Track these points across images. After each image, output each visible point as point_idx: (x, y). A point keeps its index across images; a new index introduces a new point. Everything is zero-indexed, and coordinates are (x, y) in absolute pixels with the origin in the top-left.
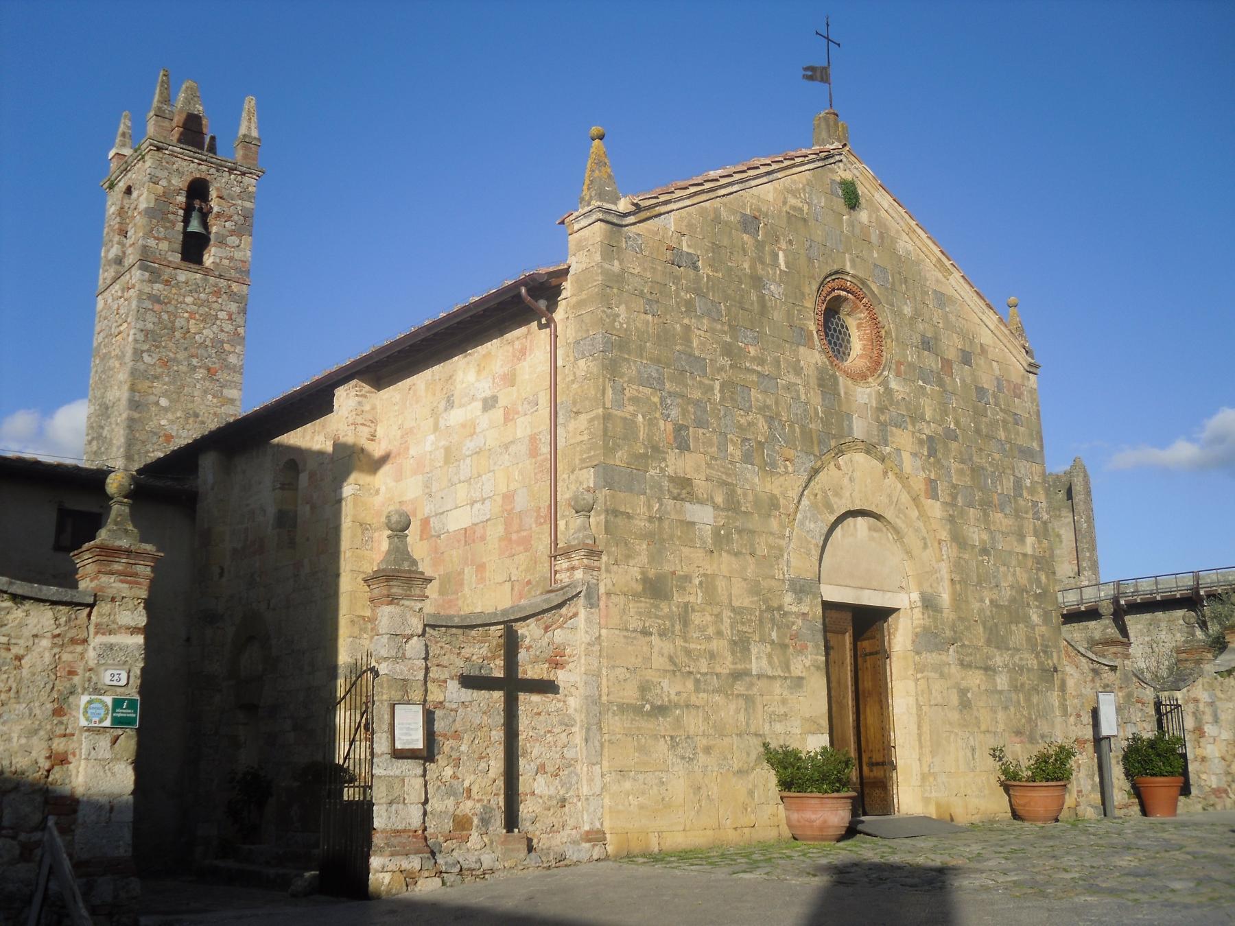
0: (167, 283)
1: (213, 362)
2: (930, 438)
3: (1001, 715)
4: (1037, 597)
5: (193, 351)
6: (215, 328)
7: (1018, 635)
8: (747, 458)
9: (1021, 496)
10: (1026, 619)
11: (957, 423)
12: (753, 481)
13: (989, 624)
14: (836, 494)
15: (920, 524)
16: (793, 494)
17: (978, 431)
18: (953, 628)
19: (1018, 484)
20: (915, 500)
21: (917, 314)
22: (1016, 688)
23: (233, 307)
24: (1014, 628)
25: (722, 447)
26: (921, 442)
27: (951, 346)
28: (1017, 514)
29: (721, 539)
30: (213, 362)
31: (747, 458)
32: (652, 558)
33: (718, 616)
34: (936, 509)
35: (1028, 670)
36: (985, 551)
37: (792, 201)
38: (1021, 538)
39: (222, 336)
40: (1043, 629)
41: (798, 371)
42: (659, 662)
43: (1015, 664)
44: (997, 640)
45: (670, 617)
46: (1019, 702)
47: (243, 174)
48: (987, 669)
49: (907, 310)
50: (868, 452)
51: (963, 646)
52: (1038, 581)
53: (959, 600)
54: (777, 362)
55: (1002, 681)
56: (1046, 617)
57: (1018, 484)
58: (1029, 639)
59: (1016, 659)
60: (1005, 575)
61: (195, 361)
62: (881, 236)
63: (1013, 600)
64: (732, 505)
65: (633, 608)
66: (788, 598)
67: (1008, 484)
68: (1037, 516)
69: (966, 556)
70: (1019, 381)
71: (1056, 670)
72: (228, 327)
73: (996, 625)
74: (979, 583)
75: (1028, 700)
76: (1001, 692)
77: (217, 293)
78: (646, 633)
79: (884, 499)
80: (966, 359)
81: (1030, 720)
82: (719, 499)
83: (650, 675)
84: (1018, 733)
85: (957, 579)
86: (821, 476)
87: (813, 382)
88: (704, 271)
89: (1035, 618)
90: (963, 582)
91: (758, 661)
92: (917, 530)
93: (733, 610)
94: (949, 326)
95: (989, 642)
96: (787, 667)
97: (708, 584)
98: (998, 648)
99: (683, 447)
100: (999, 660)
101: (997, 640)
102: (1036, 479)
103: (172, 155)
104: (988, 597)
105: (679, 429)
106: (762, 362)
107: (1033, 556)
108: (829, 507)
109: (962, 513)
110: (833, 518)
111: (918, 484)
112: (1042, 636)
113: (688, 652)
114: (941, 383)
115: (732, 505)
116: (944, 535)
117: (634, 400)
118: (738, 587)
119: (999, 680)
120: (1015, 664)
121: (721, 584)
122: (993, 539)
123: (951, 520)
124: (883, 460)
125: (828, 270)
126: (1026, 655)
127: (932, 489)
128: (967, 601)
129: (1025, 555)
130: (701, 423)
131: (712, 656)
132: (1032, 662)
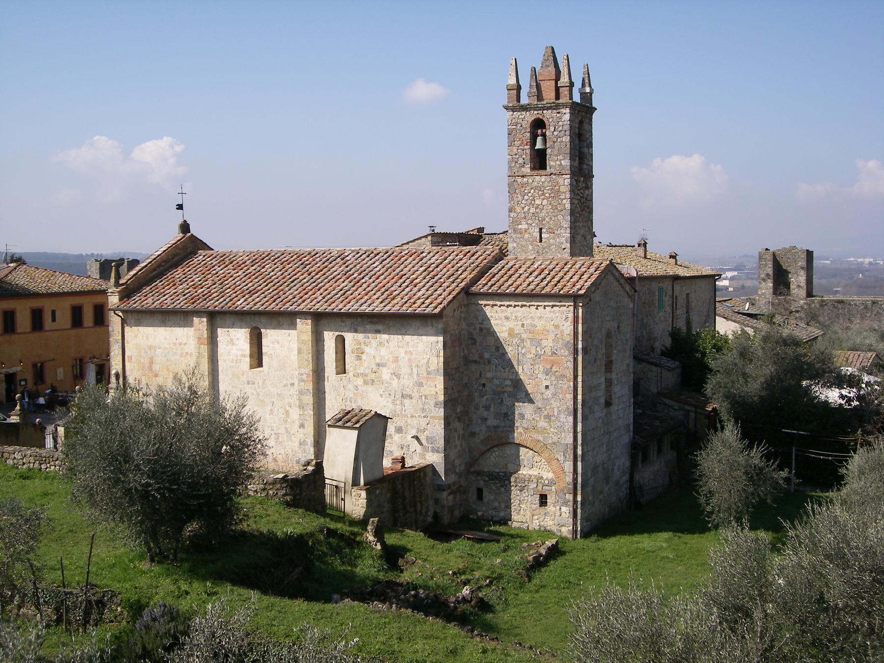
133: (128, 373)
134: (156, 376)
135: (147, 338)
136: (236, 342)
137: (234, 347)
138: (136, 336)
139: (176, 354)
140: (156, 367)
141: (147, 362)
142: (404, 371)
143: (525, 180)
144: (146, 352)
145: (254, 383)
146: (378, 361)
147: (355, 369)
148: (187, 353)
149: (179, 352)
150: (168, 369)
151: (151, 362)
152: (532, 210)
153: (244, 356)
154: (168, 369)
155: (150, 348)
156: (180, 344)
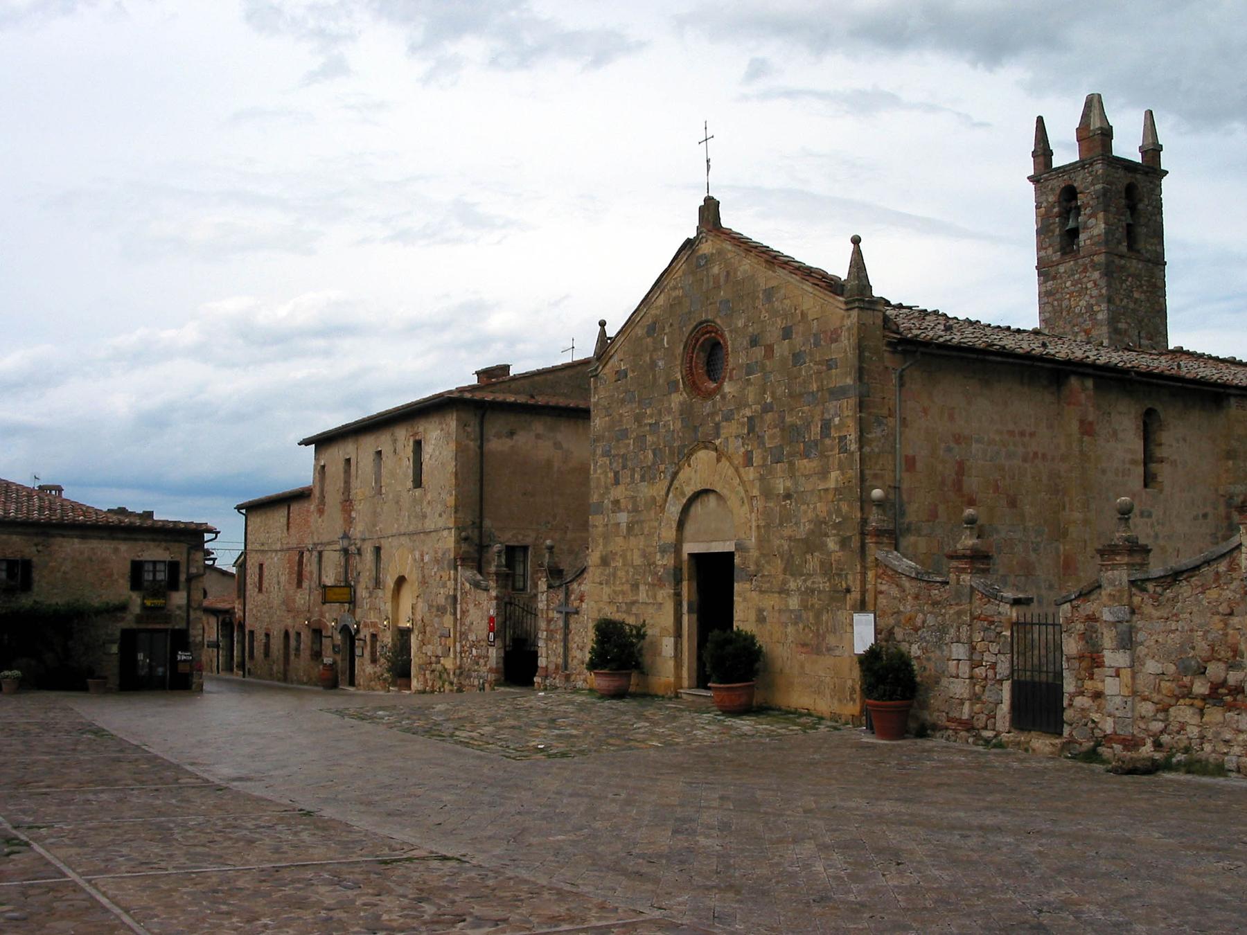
0: (1054, 278)
1: (1088, 325)
2: (750, 419)
3: (790, 629)
4: (836, 526)
5: (1075, 322)
6: (1087, 298)
7: (813, 562)
8: (643, 479)
9: (828, 436)
10: (822, 547)
11: (773, 394)
12: (647, 491)
13: (786, 557)
14: (688, 485)
15: (741, 489)
16: (663, 493)
17: (791, 395)
18: (757, 564)
19: (826, 426)
20: (737, 470)
24: (809, 557)
25: (632, 477)
26: (743, 424)
27: (773, 334)
28: (823, 456)
29: (630, 528)
30: (1088, 325)
31: (643, 479)
32: (605, 545)
33: (627, 572)
34: (750, 474)
35: (820, 592)
36: (788, 496)
37: (675, 294)
38: (824, 474)
39: (1093, 301)
40: (840, 554)
41: (669, 410)
42: (605, 598)
43: (807, 588)
44: (791, 569)
45: (609, 575)
46: (808, 619)
47: (1091, 164)
48: (779, 593)
49: (740, 324)
50: (706, 448)
51: (763, 576)
52: (838, 511)
53: (761, 541)
54: (660, 411)
55: (794, 603)
56: (844, 543)
57: (826, 426)
58: (822, 563)
59: (809, 583)
60: (805, 512)
61: (1076, 329)
62: (728, 273)
63: (812, 532)
64: (635, 510)
65: (599, 571)
66: (658, 556)
67: (816, 430)
68: (843, 449)
69: (771, 505)
70: (838, 324)
72: (1095, 292)
73: (793, 556)
74: (781, 524)
75: (818, 616)
76: (792, 611)
77: (1085, 270)
78: (601, 584)
79: (717, 478)
80: (787, 333)
81: (817, 634)
82: (630, 507)
83: (601, 605)
84: (804, 645)
85: (762, 523)
86: (681, 475)
87: (677, 414)
88: (630, 375)
89: (832, 544)
90: (767, 526)
91: (642, 596)
92: (737, 493)
93: (633, 567)
94: (774, 313)
95: (785, 571)
96: (655, 598)
97: (624, 557)
98: (792, 575)
99: (617, 482)
100: (792, 585)
101: (791, 569)
102: (846, 414)
103: (1046, 180)
105: (616, 473)
106: (651, 416)
107: (836, 489)
108: (683, 494)
109: (770, 472)
110: (684, 501)
112: (838, 562)
113: (615, 592)
114: (763, 368)
115: (635, 510)
116: (756, 492)
117: (601, 466)
118: (637, 553)
119: (791, 602)
120: (807, 588)
121: (629, 554)
122: (796, 484)
123: (762, 478)
124: (716, 450)
125: (691, 327)
127: (748, 461)
128: (769, 541)
129: (826, 490)
130: (624, 467)
131: (623, 593)
132: (822, 583)
135: (951, 418)
136: (1121, 435)
138: (925, 411)
140: (972, 483)
143: (1123, 262)
144: (949, 450)
145: (1150, 516)
148: (1036, 454)
151: (961, 469)
152: (1132, 306)
153: (1133, 462)
155: (958, 439)
156: (1022, 434)
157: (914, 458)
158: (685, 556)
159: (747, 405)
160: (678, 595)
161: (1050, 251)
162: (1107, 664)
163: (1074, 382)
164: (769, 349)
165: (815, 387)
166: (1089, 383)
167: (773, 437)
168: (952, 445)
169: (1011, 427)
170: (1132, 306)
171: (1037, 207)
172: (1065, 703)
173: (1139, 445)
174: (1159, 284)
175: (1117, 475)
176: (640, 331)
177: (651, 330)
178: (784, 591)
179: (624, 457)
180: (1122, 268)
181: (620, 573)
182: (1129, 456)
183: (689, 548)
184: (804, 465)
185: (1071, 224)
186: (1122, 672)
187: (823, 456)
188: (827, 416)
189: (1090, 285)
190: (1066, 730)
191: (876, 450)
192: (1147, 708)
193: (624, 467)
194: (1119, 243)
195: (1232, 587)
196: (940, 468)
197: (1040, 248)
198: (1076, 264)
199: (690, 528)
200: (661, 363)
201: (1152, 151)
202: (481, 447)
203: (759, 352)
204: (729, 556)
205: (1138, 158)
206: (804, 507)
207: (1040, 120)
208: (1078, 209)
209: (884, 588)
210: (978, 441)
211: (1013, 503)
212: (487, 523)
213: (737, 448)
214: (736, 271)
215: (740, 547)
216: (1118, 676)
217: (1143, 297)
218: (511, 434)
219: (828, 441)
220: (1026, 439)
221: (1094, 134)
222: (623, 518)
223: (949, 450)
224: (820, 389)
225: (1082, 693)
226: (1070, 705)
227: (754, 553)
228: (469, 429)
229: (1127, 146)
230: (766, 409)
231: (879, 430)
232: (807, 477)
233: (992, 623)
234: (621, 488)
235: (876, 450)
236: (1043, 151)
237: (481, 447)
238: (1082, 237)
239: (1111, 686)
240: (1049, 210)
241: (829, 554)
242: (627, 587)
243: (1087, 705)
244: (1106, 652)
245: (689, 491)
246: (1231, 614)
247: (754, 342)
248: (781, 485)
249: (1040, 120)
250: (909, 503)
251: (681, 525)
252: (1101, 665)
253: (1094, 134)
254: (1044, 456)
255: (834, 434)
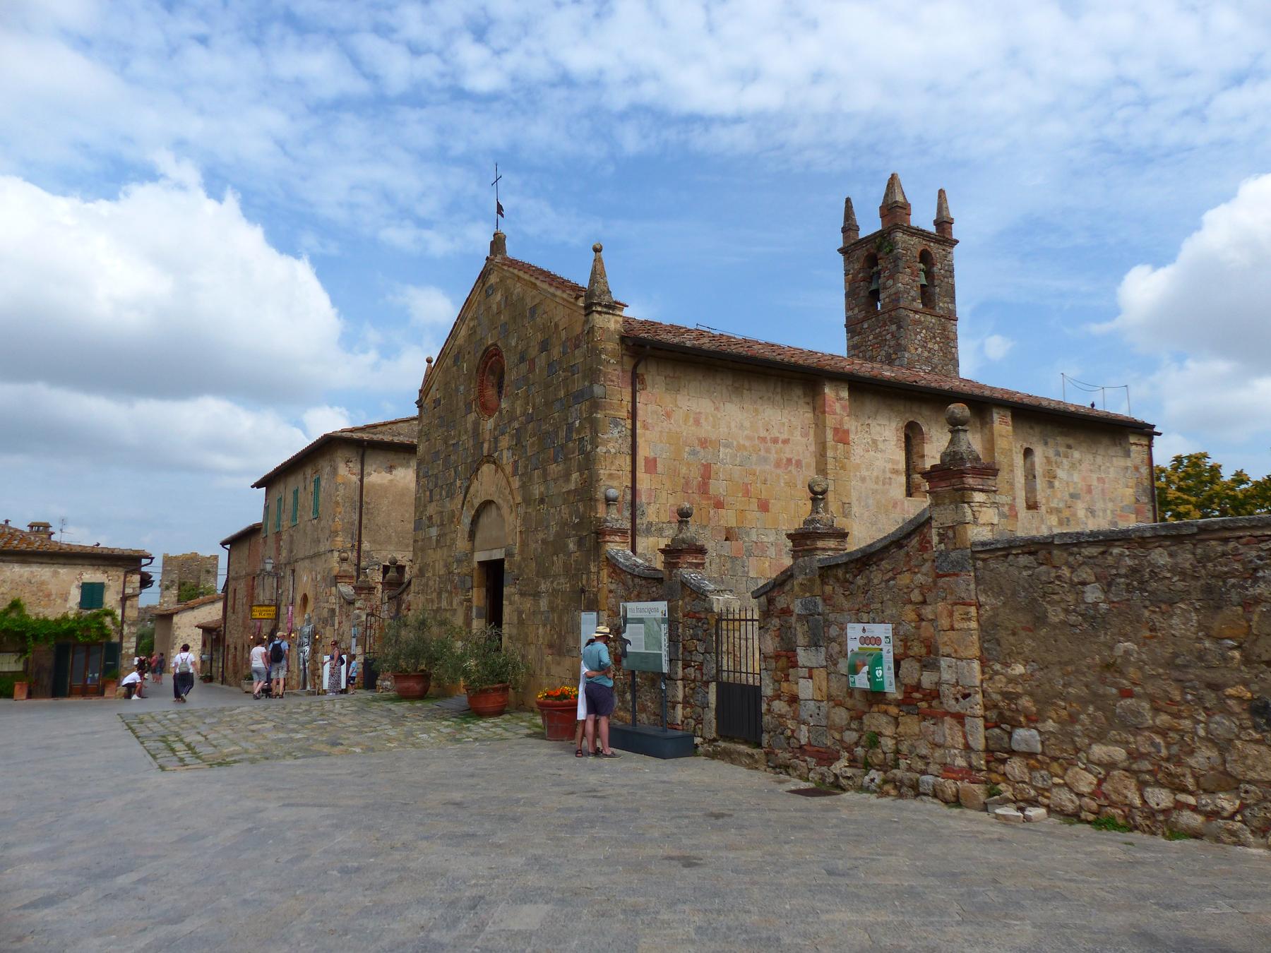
0: (859, 334)
7: (559, 561)
21: (519, 338)
22: (552, 609)
23: (894, 327)
28: (566, 459)
29: (438, 541)
34: (516, 483)
36: (542, 501)
38: (567, 476)
43: (554, 590)
55: (544, 604)
56: (580, 543)
63: (557, 534)
67: (562, 434)
68: (582, 451)
71: (583, 591)
75: (560, 618)
80: (545, 346)
81: (560, 636)
84: (551, 646)
86: (472, 490)
92: (508, 501)
98: (544, 577)
104: (540, 536)
105: (431, 491)
109: (530, 479)
111: (509, 469)
116: (519, 499)
120: (554, 590)
122: (547, 489)
123: (523, 486)
124: (494, 463)
126: (562, 580)
131: (432, 601)
133: (643, 498)
134: (719, 505)
135: (697, 422)
136: (881, 446)
137: (879, 455)
138: (668, 415)
139: (765, 460)
141: (695, 475)
142: (1099, 505)
144: (694, 453)
146: (1072, 490)
147: (1048, 501)
148: (789, 461)
149: (773, 456)
150: (747, 493)
151: (707, 473)
152: (926, 354)
153: (895, 472)
154: (747, 493)
155: (704, 443)
156: (775, 441)
157: (655, 460)
158: (476, 565)
159: (517, 419)
160: (469, 600)
161: (856, 311)
162: (800, 664)
163: (828, 391)
164: (533, 361)
165: (562, 394)
166: (845, 394)
167: (533, 444)
168: (698, 448)
169: (763, 434)
170: (926, 354)
171: (846, 275)
172: (764, 707)
173: (901, 456)
174: (952, 336)
175: (877, 483)
176: (449, 361)
177: (457, 359)
178: (536, 595)
179: (436, 476)
180: (918, 322)
181: (431, 583)
182: (889, 466)
183: (480, 556)
184: (553, 468)
185: (874, 287)
186: (815, 672)
187: (566, 459)
188: (570, 421)
189: (889, 337)
190: (765, 738)
191: (613, 451)
192: (841, 716)
193: (436, 486)
194: (914, 300)
195: (924, 569)
196: (684, 470)
197: (849, 308)
198: (877, 320)
199: (479, 536)
200: (462, 388)
201: (943, 223)
202: (361, 480)
203: (524, 367)
204: (501, 562)
205: (932, 229)
206: (552, 510)
207: (848, 201)
208: (879, 273)
209: (613, 587)
210: (726, 446)
211: (764, 507)
212: (366, 546)
213: (507, 457)
214: (512, 294)
215: (509, 554)
216: (811, 677)
217: (936, 347)
218: (390, 469)
219: (571, 445)
220: (780, 445)
221: (894, 210)
222: (434, 532)
223: (694, 453)
224: (567, 395)
225: (778, 697)
226: (769, 710)
227: (517, 558)
228: (351, 465)
229: (923, 218)
230: (530, 419)
231: (616, 431)
232: (555, 480)
233: (699, 619)
234: (434, 504)
235: (613, 451)
236: (849, 227)
237: (361, 480)
238: (882, 296)
239: (805, 689)
240: (855, 276)
241: (570, 555)
242: (434, 595)
243: (783, 711)
244: (800, 651)
245: (477, 503)
246: (924, 602)
247: (522, 359)
248: (537, 490)
249: (848, 201)
250: (649, 504)
251: (472, 535)
252: (795, 665)
253: (894, 210)
254: (799, 463)
255: (575, 436)
